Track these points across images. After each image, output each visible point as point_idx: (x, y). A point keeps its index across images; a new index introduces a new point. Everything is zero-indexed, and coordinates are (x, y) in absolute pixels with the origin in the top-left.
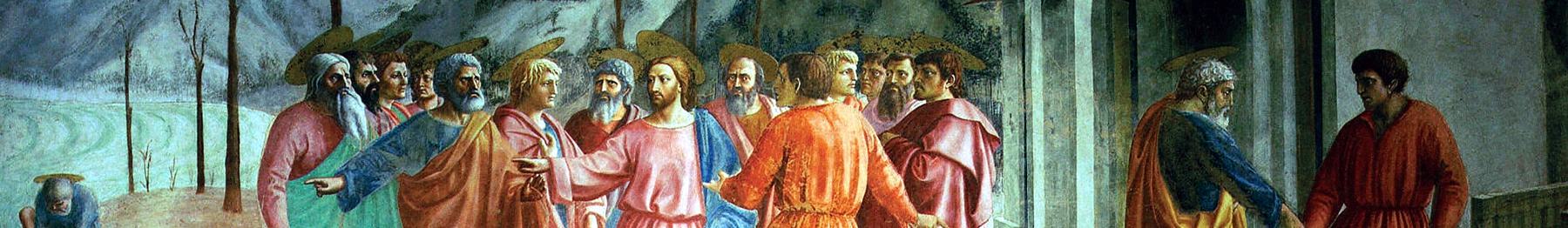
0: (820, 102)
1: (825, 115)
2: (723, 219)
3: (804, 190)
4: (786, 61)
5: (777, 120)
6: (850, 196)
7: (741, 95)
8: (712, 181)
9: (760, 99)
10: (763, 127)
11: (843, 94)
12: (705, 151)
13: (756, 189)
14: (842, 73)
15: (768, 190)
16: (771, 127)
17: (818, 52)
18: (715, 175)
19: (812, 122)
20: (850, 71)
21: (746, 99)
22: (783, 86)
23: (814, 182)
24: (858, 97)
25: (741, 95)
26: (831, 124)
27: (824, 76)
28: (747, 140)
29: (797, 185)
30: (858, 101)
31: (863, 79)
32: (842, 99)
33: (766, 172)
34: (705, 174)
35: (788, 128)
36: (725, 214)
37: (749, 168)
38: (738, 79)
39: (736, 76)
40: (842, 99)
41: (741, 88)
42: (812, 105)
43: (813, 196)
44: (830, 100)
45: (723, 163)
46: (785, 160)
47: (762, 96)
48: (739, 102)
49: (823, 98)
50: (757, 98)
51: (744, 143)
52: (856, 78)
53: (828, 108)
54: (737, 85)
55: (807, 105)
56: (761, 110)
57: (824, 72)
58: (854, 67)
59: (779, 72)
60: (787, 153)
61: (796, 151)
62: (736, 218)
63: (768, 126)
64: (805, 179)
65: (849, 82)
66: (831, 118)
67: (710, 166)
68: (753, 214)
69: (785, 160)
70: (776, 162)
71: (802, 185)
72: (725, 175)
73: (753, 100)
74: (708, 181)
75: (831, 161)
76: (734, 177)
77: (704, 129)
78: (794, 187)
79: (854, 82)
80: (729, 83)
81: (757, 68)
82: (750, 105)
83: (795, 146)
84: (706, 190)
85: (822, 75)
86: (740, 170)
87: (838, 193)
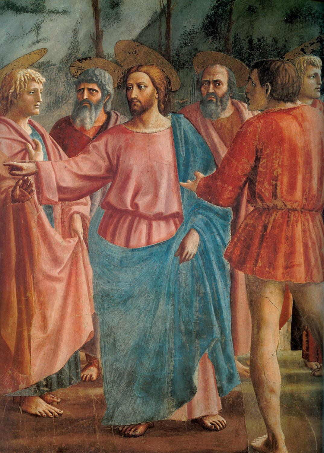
0: (290, 105)
1: (295, 117)
2: (200, 216)
3: (276, 188)
4: (258, 68)
5: (249, 123)
6: (318, 193)
7: (214, 100)
8: (189, 181)
9: (233, 104)
10: (236, 130)
11: (311, 98)
12: (182, 153)
13: (230, 188)
14: (309, 77)
15: (242, 189)
16: (244, 129)
17: (286, 58)
18: (192, 175)
19: (283, 124)
21: (219, 103)
22: (254, 90)
23: (285, 180)
25: (214, 100)
26: (300, 125)
28: (221, 142)
29: (270, 184)
32: (310, 102)
33: (239, 172)
34: (182, 174)
35: (259, 130)
36: (200, 211)
37: (224, 168)
38: (211, 86)
39: (209, 82)
40: (310, 102)
41: (215, 94)
42: (283, 108)
43: (285, 193)
45: (199, 163)
46: (258, 159)
47: (235, 101)
48: (213, 107)
50: (229, 103)
51: (218, 146)
53: (298, 111)
54: (211, 90)
55: (277, 108)
56: (233, 113)
59: (250, 78)
60: (259, 154)
61: (268, 151)
62: (211, 215)
63: (241, 128)
64: (277, 177)
66: (300, 119)
67: (187, 166)
68: (227, 212)
69: (258, 159)
70: (248, 162)
71: (274, 182)
72: (201, 175)
73: (227, 105)
74: (185, 180)
75: (301, 160)
76: (209, 176)
77: (180, 132)
78: (266, 185)
80: (203, 89)
81: (228, 74)
82: (224, 109)
83: (267, 147)
84: (182, 188)
85: (291, 80)
86: (215, 170)
87: (307, 190)
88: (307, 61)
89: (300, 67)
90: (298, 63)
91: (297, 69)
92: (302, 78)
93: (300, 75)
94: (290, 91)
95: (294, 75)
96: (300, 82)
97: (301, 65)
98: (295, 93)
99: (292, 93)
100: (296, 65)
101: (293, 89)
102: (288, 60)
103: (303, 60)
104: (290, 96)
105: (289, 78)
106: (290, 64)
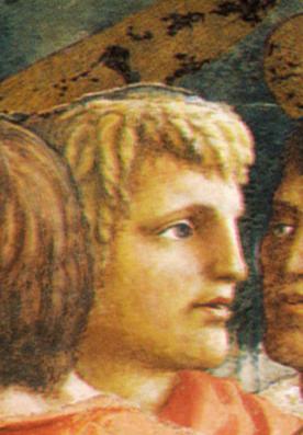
11: (155, 360)
14: (153, 231)
20: (199, 222)
24: (247, 375)
27: (47, 251)
30: (249, 401)
31: (281, 274)
32: (152, 388)
40: (152, 388)
44: (77, 390)
49: (40, 380)
52: (238, 266)
57: (44, 232)
58: (227, 200)
65: (196, 288)
79: (226, 291)
88: (140, 131)
89: (96, 166)
90: (84, 141)
91: (77, 176)
92: (105, 234)
93: (89, 216)
94: (27, 315)
95: (55, 218)
96: (91, 260)
97: (98, 153)
98: (59, 330)
99: (40, 328)
100: (71, 151)
101: (46, 302)
102: (21, 119)
103: (116, 119)
104: (28, 349)
105: (21, 235)
106: (35, 147)
